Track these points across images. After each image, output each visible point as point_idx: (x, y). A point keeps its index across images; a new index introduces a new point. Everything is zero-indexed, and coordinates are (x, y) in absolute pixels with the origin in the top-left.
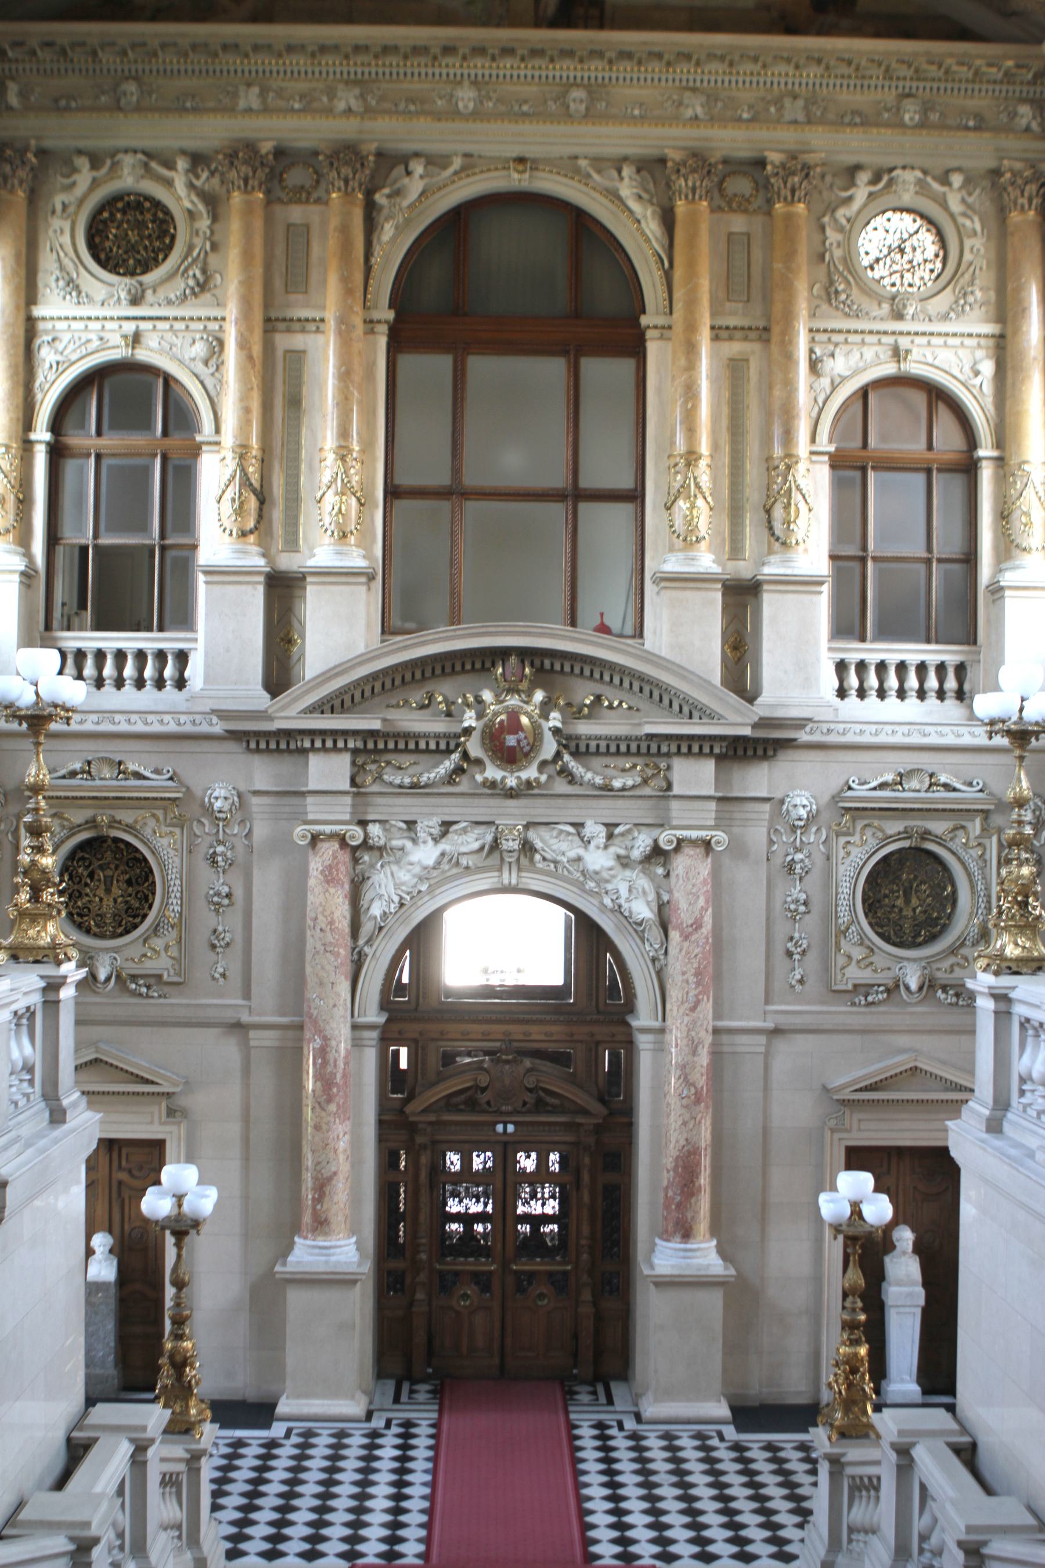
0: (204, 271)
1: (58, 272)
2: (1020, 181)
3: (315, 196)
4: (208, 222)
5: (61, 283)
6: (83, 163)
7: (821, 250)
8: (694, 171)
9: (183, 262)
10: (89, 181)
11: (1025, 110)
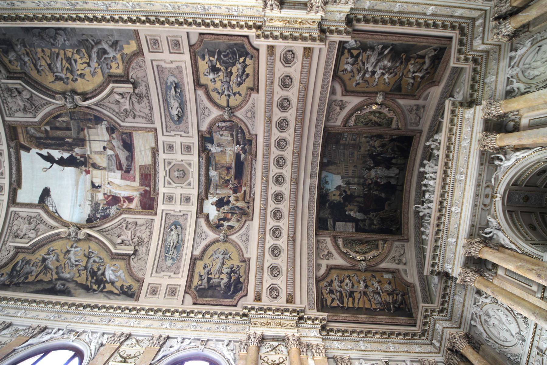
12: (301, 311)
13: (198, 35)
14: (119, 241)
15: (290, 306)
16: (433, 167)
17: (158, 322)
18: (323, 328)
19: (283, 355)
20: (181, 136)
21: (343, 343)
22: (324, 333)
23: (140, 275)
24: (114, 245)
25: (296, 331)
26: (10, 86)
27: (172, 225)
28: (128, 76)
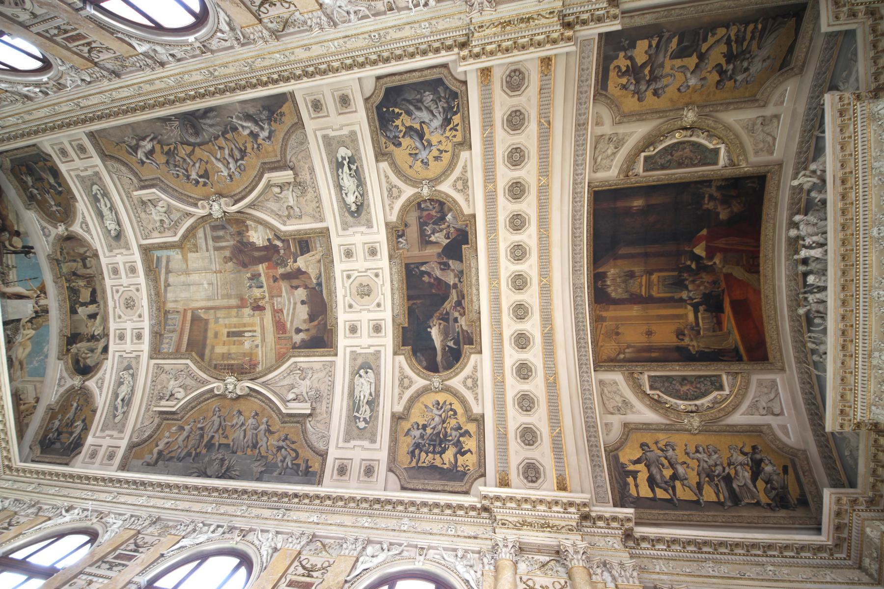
12: (585, 505)
13: (374, 80)
14: (291, 396)
15: (564, 496)
16: (815, 225)
17: (350, 517)
18: (628, 535)
19: (561, 577)
20: (362, 233)
21: (672, 563)
22: (631, 544)
23: (320, 446)
24: (285, 402)
25: (580, 538)
27: (360, 369)
28: (286, 161)
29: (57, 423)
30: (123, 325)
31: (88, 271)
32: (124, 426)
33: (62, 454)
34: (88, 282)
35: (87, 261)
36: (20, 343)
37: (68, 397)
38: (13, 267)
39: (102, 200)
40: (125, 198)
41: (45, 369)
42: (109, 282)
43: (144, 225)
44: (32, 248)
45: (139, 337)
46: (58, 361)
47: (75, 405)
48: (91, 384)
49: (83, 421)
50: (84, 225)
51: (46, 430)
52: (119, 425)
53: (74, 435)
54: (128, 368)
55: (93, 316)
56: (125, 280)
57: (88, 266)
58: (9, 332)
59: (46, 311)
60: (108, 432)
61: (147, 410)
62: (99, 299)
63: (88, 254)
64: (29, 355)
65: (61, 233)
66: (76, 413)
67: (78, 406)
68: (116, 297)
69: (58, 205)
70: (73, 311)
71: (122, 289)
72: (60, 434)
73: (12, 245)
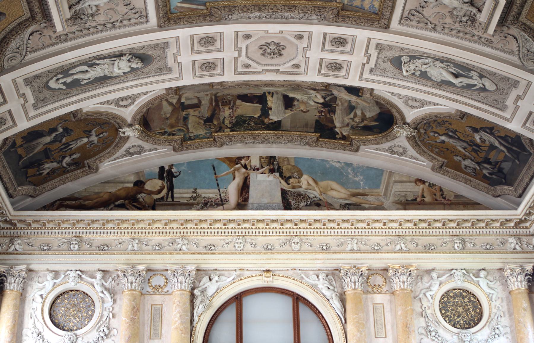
0: (108, 328)
1: (33, 329)
2: (515, 274)
3: (165, 290)
4: (112, 303)
5: (35, 335)
6: (50, 276)
7: (421, 310)
8: (354, 274)
9: (98, 323)
10: (52, 284)
11: (512, 240)
26: (68, 14)
29: (468, 162)
30: (314, 62)
31: (205, 102)
32: (506, 79)
33: (525, 162)
34: (226, 103)
35: (187, 103)
36: (321, 193)
37: (425, 144)
38: (195, 192)
39: (76, 77)
40: (69, 44)
41: (369, 168)
42: (228, 76)
43: (119, 17)
44: (162, 169)
45: (340, 42)
46: (360, 152)
47: (443, 138)
48: (411, 115)
49: (476, 130)
50: (121, 103)
51: (475, 177)
52: (501, 85)
53: (497, 144)
54: (397, 63)
55: (288, 103)
56: (228, 54)
57: (195, 101)
58: (302, 204)
59: (271, 160)
60: (510, 102)
61: (488, 42)
62: (258, 92)
63: (174, 101)
64: (343, 184)
65: (137, 134)
66: (459, 139)
67: (447, 135)
68: (259, 68)
69: (88, 133)
70: (277, 126)
71: (243, 59)
72: (487, 161)
73: (159, 192)
